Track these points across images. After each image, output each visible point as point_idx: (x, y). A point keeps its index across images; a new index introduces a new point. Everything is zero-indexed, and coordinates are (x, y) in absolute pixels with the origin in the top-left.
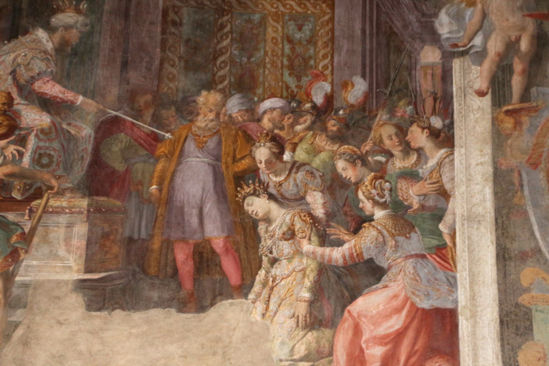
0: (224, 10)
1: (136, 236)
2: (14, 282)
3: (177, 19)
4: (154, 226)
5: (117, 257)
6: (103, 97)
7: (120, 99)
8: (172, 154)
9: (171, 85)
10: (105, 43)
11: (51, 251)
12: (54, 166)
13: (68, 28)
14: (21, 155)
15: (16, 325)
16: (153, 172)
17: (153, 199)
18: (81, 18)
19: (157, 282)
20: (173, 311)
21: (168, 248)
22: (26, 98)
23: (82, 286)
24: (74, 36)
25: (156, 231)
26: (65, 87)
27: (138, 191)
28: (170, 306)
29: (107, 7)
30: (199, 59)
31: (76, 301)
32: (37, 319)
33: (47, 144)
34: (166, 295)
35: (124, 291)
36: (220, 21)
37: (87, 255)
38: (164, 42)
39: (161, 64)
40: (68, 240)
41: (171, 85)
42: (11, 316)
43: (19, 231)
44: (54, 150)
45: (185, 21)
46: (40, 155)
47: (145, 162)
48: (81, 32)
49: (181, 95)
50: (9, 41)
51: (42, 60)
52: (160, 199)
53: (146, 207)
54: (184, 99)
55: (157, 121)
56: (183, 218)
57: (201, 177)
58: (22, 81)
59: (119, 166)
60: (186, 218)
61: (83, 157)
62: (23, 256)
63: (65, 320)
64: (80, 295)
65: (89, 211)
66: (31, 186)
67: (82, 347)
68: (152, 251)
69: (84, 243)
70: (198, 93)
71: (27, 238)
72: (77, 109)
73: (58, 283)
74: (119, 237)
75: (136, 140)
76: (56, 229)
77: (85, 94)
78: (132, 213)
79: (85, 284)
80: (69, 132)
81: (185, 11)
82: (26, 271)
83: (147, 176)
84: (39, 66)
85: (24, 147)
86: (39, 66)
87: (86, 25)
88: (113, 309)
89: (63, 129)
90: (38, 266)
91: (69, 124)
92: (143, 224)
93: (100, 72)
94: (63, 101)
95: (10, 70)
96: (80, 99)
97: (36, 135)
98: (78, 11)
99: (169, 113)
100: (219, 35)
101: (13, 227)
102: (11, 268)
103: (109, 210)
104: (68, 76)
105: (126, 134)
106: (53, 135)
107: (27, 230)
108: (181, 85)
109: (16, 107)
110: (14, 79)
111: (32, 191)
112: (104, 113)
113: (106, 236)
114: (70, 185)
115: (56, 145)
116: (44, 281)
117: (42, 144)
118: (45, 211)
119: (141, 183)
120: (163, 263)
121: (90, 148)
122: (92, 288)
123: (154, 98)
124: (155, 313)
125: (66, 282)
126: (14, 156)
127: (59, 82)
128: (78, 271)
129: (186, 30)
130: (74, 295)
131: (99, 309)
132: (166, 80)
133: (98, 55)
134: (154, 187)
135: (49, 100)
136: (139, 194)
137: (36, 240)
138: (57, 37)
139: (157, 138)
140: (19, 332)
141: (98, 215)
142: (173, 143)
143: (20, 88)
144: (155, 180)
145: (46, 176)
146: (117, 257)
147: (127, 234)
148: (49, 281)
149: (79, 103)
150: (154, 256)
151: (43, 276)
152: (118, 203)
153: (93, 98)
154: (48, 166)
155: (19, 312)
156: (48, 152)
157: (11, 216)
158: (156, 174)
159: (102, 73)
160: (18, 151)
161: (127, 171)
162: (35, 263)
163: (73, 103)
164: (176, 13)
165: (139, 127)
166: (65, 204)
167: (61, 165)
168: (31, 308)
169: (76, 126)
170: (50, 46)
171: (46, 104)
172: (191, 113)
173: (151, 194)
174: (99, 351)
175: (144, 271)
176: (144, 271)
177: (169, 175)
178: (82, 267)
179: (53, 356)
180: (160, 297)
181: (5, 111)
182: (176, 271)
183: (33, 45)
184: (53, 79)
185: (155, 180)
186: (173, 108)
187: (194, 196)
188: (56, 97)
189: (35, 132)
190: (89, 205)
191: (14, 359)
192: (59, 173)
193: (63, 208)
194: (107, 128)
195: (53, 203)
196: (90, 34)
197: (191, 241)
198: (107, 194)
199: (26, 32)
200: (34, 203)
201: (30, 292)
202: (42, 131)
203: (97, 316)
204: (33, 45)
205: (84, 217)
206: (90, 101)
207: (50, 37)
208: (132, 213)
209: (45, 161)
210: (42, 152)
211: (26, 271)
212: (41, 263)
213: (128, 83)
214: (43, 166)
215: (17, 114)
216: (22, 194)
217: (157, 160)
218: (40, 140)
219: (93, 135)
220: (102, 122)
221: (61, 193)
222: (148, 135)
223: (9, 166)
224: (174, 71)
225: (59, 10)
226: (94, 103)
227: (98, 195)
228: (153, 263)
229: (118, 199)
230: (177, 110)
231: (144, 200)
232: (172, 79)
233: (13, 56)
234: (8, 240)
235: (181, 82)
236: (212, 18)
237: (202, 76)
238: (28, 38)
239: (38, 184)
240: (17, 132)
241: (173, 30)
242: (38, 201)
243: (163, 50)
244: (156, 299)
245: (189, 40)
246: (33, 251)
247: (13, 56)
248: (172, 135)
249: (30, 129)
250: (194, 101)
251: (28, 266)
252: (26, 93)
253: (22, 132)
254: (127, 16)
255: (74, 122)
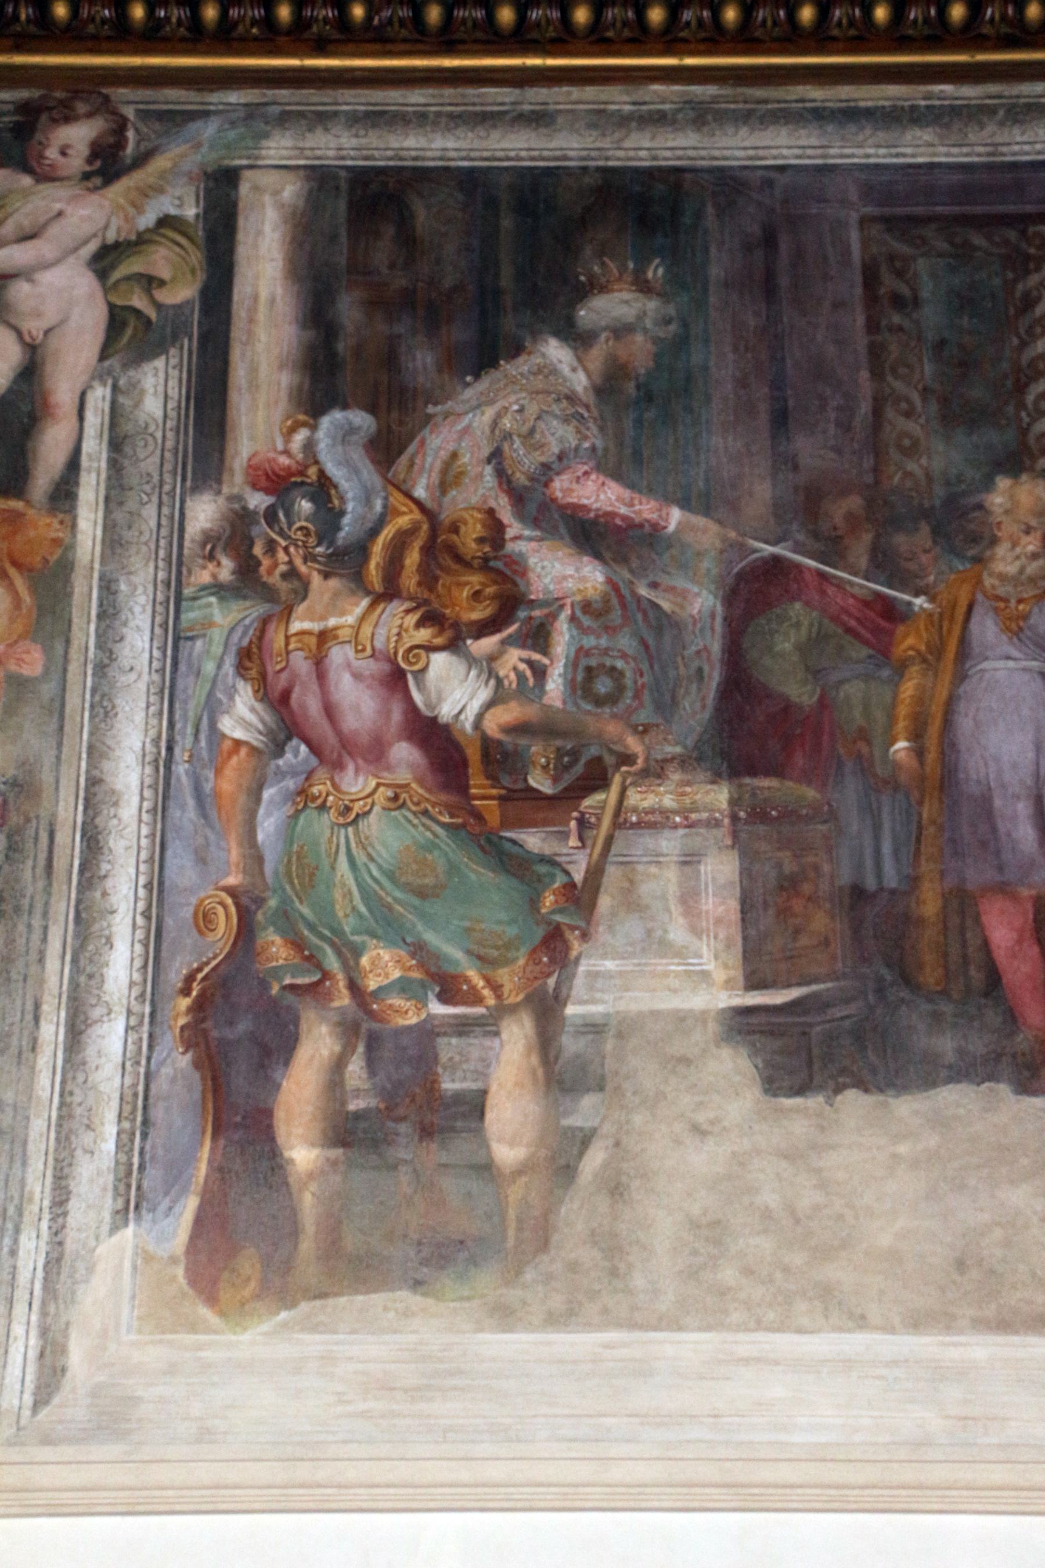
0: (1028, 258)
1: (870, 883)
2: (564, 1018)
3: (905, 291)
4: (917, 853)
5: (826, 943)
6: (734, 507)
7: (778, 509)
8: (938, 650)
9: (911, 466)
10: (721, 365)
11: (649, 932)
12: (628, 699)
13: (621, 331)
14: (540, 673)
15: (585, 1139)
16: (894, 705)
17: (903, 778)
18: (652, 305)
19: (947, 1008)
20: (1004, 1089)
21: (962, 913)
22: (535, 523)
23: (743, 1025)
24: (639, 352)
25: (925, 867)
26: (632, 486)
27: (859, 756)
28: (990, 1078)
29: (715, 272)
30: (978, 393)
31: (732, 1067)
32: (638, 1119)
33: (604, 642)
34: (978, 1045)
35: (859, 1037)
36: (1020, 287)
37: (745, 938)
38: (876, 352)
39: (877, 412)
40: (689, 899)
41: (911, 466)
42: (567, 1114)
43: (560, 880)
44: (624, 656)
45: (925, 294)
46: (589, 669)
47: (867, 678)
48: (656, 341)
49: (940, 491)
50: (477, 376)
51: (566, 420)
52: (923, 778)
53: (886, 800)
54: (951, 501)
55: (885, 564)
56: (994, 829)
57: (1026, 712)
58: (521, 479)
59: (800, 693)
60: (1002, 827)
61: (700, 670)
62: (576, 947)
63: (712, 1123)
64: (744, 1052)
65: (734, 818)
66: (575, 754)
67: (770, 1198)
68: (921, 921)
69: (734, 905)
70: (988, 484)
71: (582, 898)
72: (670, 542)
73: (680, 1018)
74: (824, 886)
75: (835, 619)
76: (653, 869)
77: (685, 504)
78: (854, 823)
79: (753, 1020)
80: (656, 606)
81: (922, 265)
82: (591, 988)
83: (879, 715)
84: (559, 435)
85: (545, 651)
86: (559, 435)
87: (668, 321)
88: (838, 1090)
89: (639, 599)
90: (621, 974)
91: (654, 585)
92: (887, 848)
93: (717, 440)
94: (632, 525)
95: (486, 452)
96: (675, 516)
97: (573, 619)
98: (644, 287)
99: (914, 542)
100: (1023, 324)
101: (542, 869)
102: (551, 982)
103: (789, 815)
104: (637, 457)
105: (807, 604)
106: (616, 616)
107: (578, 877)
108: (937, 465)
109: (511, 547)
110: (500, 473)
111: (579, 769)
112: (743, 550)
113: (789, 885)
114: (678, 749)
115: (626, 642)
116: (641, 1014)
117: (589, 642)
118: (619, 822)
119: (863, 735)
120: (954, 950)
121: (716, 648)
122: (771, 1032)
123: (870, 503)
124: (955, 1098)
125: (702, 1017)
126: (521, 677)
127: (617, 476)
128: (728, 984)
129: (932, 317)
130: (726, 1053)
131: (800, 1090)
132: (894, 455)
133: (708, 399)
134: (902, 744)
135: (595, 522)
136: (864, 767)
137: (605, 902)
138: (597, 355)
139: (891, 613)
140: (594, 1159)
141: (762, 829)
142: (937, 622)
143: (518, 498)
144: (901, 725)
145: (609, 728)
146: (826, 943)
147: (845, 877)
148: (655, 1014)
149: (672, 527)
150: (930, 934)
151: (639, 1000)
152: (810, 793)
153: (707, 511)
154: (612, 699)
155: (588, 1101)
156: (608, 662)
157: (533, 840)
158: (903, 710)
159: (723, 444)
160: (530, 663)
161: (823, 704)
162: (610, 965)
163: (657, 527)
164: (900, 274)
165: (840, 585)
166: (668, 801)
167: (646, 697)
168: (618, 1088)
169: (672, 589)
170: (580, 382)
171: (589, 534)
172: (975, 539)
173: (896, 766)
174: (817, 1208)
175: (907, 980)
176: (907, 980)
177: (936, 710)
178: (738, 974)
179: (694, 1225)
180: (961, 1052)
181: (486, 559)
182: (994, 978)
183: (539, 383)
184: (600, 468)
185: (901, 725)
186: (925, 529)
187: (1015, 766)
188: (613, 515)
189: (568, 611)
190: (733, 802)
191: (593, 1233)
192: (644, 716)
193: (665, 813)
194: (756, 590)
195: (639, 799)
196: (681, 343)
197: (1025, 892)
198: (777, 771)
199: (517, 350)
200: (590, 802)
201: (609, 1046)
202: (587, 606)
203: (798, 1110)
204: (539, 383)
205: (723, 835)
206: (700, 521)
207: (580, 360)
208: (854, 823)
209: (603, 686)
210: (593, 662)
211: (591, 988)
212: (628, 966)
213: (796, 468)
214: (599, 701)
215: (517, 567)
216: (555, 780)
217: (901, 669)
218: (584, 631)
219: (719, 609)
220: (740, 576)
221: (654, 772)
222: (866, 604)
223: (513, 704)
224: (913, 427)
225: (595, 287)
226: (713, 527)
227: (753, 772)
228: (929, 957)
229: (809, 783)
230: (936, 532)
231: (881, 782)
232: (912, 450)
233: (489, 413)
234: (534, 904)
235: (938, 457)
236: (997, 281)
237: (995, 438)
238: (522, 366)
239: (594, 751)
240: (522, 614)
241: (896, 319)
242: (599, 797)
243: (877, 374)
244: (950, 1057)
245: (941, 344)
246: (601, 933)
247: (489, 413)
248: (932, 599)
249: (555, 604)
250: (980, 507)
251: (594, 975)
252: (532, 508)
253: (537, 613)
254: (769, 289)
255: (665, 580)
